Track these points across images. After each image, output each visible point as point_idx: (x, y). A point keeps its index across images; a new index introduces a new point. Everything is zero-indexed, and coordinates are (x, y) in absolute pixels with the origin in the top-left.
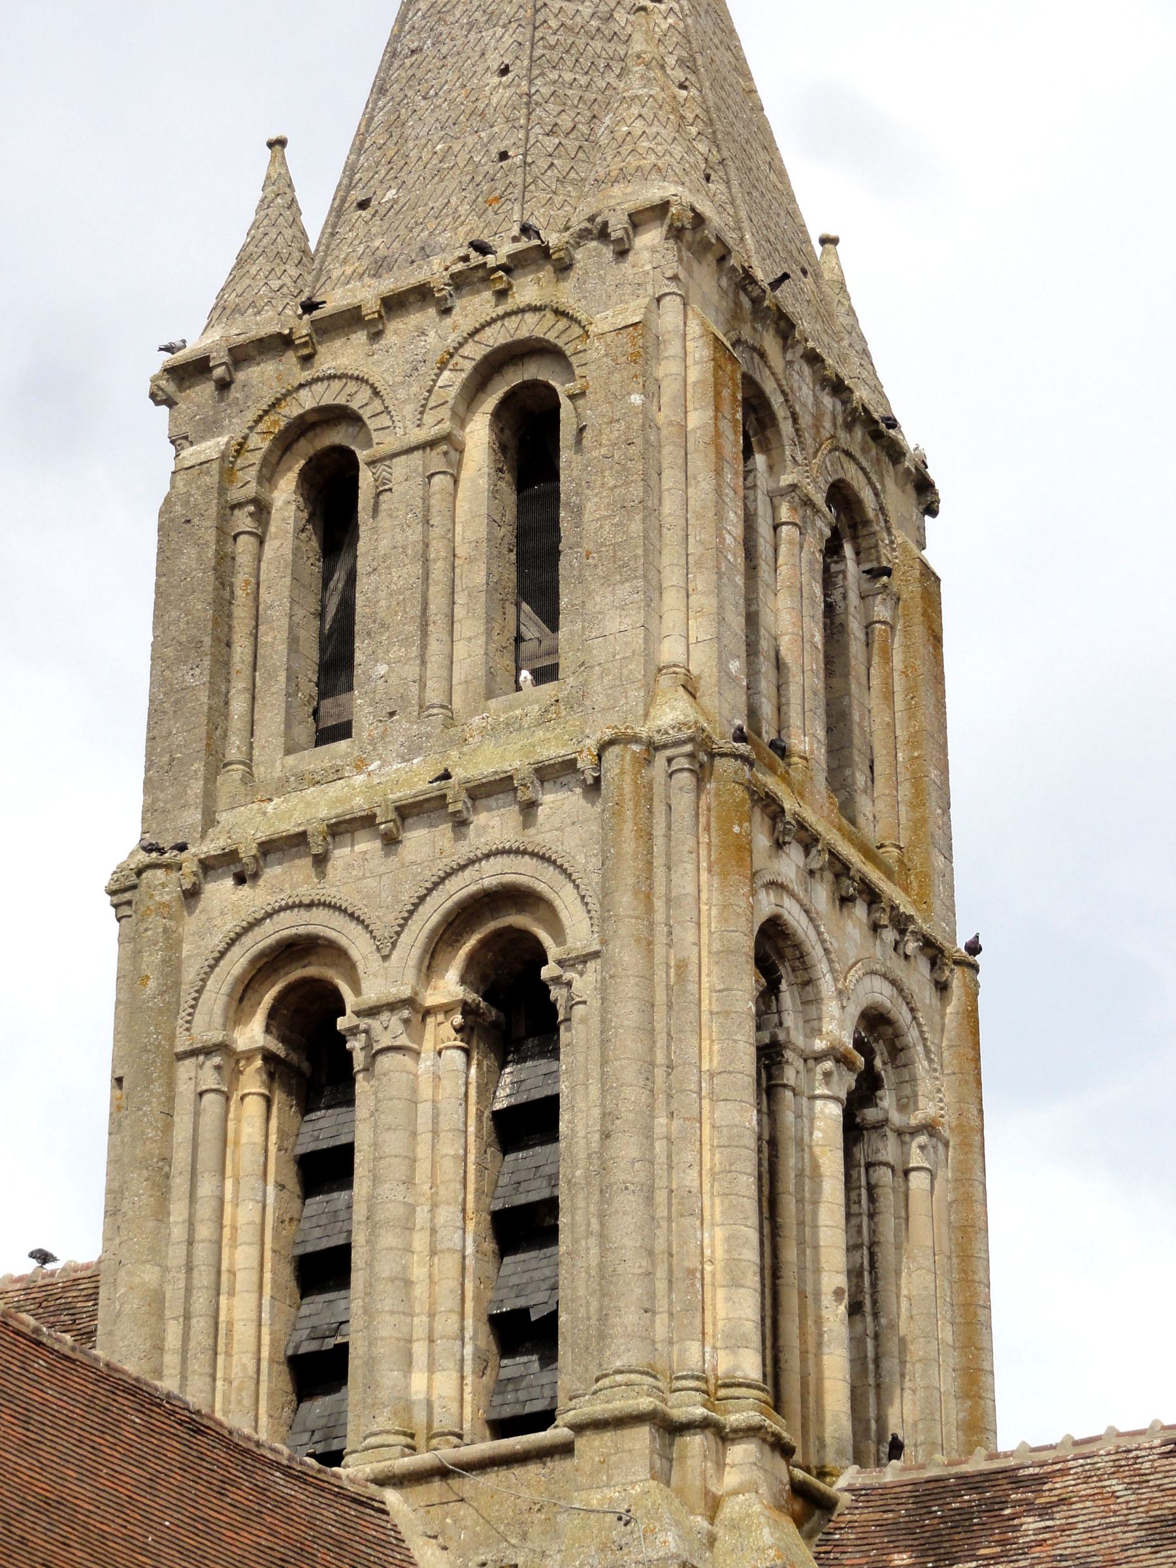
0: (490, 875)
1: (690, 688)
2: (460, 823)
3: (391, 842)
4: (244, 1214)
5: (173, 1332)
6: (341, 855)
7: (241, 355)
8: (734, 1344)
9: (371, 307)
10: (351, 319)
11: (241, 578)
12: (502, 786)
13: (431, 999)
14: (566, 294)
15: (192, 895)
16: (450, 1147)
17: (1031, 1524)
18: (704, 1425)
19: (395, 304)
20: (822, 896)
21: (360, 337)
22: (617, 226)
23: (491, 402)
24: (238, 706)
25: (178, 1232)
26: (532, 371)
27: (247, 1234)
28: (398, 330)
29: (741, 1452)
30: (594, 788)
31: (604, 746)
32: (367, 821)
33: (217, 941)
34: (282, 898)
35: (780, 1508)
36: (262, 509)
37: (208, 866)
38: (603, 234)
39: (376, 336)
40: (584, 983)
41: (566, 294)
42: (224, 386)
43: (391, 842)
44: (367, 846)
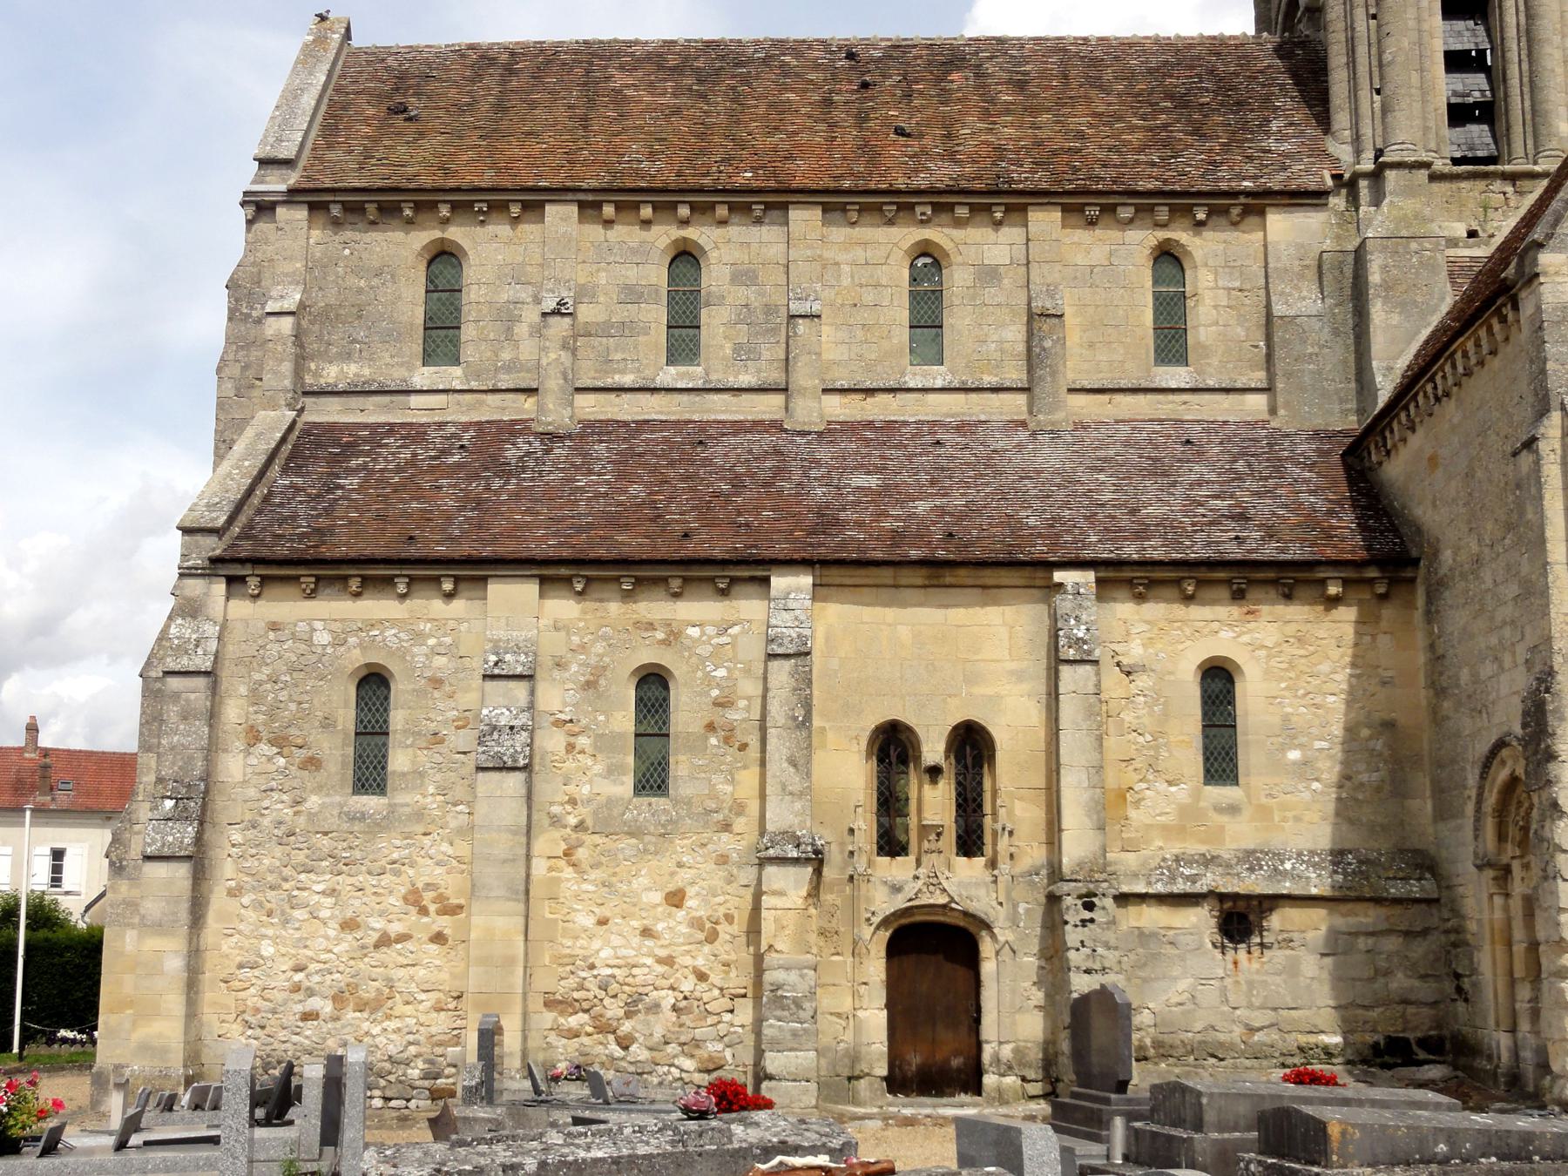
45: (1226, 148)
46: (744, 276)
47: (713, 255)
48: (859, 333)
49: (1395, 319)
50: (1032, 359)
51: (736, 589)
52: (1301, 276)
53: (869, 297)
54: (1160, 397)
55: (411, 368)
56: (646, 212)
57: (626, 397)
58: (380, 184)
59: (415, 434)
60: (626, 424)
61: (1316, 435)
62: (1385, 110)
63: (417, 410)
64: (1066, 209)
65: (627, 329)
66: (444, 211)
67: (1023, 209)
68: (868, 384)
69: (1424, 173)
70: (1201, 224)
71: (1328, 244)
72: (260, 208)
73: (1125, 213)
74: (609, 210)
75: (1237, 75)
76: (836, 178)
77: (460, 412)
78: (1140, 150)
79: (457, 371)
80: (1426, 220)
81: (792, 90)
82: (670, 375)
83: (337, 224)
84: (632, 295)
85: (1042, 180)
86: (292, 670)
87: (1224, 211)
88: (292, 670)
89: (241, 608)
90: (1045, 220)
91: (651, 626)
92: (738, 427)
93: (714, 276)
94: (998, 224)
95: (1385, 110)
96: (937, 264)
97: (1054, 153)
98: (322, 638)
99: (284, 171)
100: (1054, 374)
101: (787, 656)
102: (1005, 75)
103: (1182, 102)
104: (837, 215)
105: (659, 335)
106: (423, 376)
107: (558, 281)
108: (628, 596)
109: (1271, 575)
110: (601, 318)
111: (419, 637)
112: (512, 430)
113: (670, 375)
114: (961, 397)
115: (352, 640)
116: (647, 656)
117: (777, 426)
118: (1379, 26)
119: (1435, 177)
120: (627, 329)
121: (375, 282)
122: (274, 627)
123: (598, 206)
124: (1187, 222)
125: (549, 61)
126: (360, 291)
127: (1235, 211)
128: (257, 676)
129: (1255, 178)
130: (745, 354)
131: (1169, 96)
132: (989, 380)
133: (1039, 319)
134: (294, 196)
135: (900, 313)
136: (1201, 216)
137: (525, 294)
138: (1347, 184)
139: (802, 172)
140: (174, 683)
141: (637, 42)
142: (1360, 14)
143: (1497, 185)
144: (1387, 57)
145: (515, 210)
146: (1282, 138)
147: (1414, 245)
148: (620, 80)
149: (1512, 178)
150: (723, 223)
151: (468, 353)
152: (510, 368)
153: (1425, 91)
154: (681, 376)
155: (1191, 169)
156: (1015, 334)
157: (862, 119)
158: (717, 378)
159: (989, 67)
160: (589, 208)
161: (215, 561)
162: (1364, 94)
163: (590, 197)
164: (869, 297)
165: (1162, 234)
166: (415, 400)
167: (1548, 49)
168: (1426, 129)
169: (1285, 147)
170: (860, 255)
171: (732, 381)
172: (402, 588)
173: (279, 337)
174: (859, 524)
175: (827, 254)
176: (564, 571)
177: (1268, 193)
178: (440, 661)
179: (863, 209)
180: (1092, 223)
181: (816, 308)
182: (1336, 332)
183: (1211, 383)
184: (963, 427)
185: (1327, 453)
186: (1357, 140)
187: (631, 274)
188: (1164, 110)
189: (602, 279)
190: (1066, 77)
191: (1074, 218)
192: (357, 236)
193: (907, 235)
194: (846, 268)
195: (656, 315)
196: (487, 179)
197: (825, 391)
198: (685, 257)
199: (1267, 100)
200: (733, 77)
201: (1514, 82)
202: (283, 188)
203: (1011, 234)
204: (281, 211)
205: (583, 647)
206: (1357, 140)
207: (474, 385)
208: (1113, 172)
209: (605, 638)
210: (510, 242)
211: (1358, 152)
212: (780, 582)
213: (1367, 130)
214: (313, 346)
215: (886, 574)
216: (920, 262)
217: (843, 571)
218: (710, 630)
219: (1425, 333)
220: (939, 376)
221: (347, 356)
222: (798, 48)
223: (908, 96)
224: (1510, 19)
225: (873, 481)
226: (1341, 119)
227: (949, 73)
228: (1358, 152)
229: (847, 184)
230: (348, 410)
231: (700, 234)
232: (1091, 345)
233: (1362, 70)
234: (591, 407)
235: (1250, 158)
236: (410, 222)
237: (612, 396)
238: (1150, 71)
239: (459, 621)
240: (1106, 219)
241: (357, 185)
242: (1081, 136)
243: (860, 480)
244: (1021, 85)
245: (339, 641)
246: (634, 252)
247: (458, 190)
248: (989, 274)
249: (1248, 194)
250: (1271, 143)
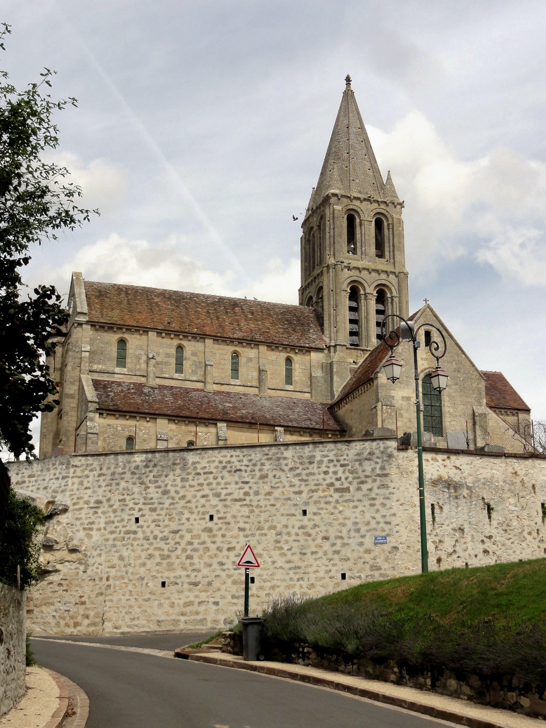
0: (383, 282)
2: (379, 274)
3: (370, 273)
6: (363, 272)
7: (343, 196)
9: (362, 199)
10: (358, 199)
12: (386, 272)
14: (388, 209)
15: (342, 270)
21: (359, 202)
22: (396, 204)
23: (375, 218)
26: (380, 216)
28: (365, 203)
30: (397, 276)
31: (400, 273)
32: (368, 270)
34: (355, 275)
37: (345, 267)
38: (393, 203)
39: (361, 202)
40: (396, 300)
41: (388, 209)
42: (339, 199)
43: (370, 273)
44: (366, 272)
45: (301, 336)
46: (194, 354)
47: (187, 348)
48: (220, 370)
49: (339, 380)
50: (260, 380)
51: (210, 425)
52: (318, 368)
53: (223, 362)
54: (286, 392)
56: (172, 336)
57: (166, 380)
58: (109, 322)
59: (119, 384)
60: (168, 386)
61: (321, 404)
62: (337, 332)
63: (117, 378)
64: (268, 346)
65: (167, 364)
66: (124, 330)
67: (258, 345)
68: (222, 383)
69: (345, 347)
70: (297, 353)
71: (324, 361)
73: (280, 349)
74: (164, 335)
75: (301, 317)
76: (216, 333)
77: (127, 380)
78: (283, 334)
79: (125, 369)
80: (345, 358)
81: (199, 308)
82: (176, 376)
83: (97, 330)
84: (168, 355)
85: (262, 339)
86: (113, 435)
87: (302, 351)
88: (113, 435)
89: (102, 420)
90: (263, 349)
91: (191, 432)
92: (195, 390)
93: (187, 353)
94: (252, 348)
95: (337, 332)
96: (237, 355)
97: (264, 332)
98: (119, 428)
99: (85, 316)
100: (265, 384)
101: (223, 440)
102: (248, 310)
103: (290, 323)
104: (216, 342)
105: (173, 366)
106: (117, 370)
107: (152, 350)
108: (186, 425)
109: (318, 432)
110: (161, 360)
112: (141, 385)
113: (176, 376)
114: (243, 387)
115: (126, 430)
117: (202, 390)
118: (336, 313)
119: (347, 348)
120: (167, 364)
121: (106, 345)
122: (109, 425)
123: (161, 333)
124: (293, 352)
125: (136, 292)
126: (102, 347)
127: (304, 351)
128: (105, 436)
129: (308, 344)
130: (194, 372)
131: (287, 321)
132: (249, 384)
133: (261, 372)
134: (87, 322)
135: (229, 366)
136: (297, 351)
137: (143, 353)
138: (329, 348)
139: (208, 330)
140: (90, 435)
141: (157, 289)
142: (332, 309)
143: (359, 352)
144: (338, 320)
145: (141, 332)
146: (313, 334)
147: (343, 364)
148: (156, 300)
149: (363, 350)
150: (190, 340)
151: (128, 365)
152: (139, 370)
153: (345, 329)
154: (180, 376)
155: (294, 339)
156: (255, 374)
157: (218, 318)
158: (188, 377)
159: (244, 307)
160: (159, 333)
161: (97, 409)
162: (332, 327)
163: (160, 331)
164: (223, 362)
165: (288, 355)
166: (116, 376)
167: (371, 322)
168: (345, 337)
169: (314, 337)
170: (221, 351)
171: (191, 379)
172: (138, 419)
173: (85, 357)
174: (233, 414)
175: (214, 351)
176: (174, 418)
177: (312, 348)
178: (146, 436)
179: (223, 341)
180: (273, 350)
181: (212, 363)
182: (325, 381)
183: (298, 390)
184: (244, 395)
185: (324, 408)
186: (330, 337)
187: (168, 350)
188: (286, 324)
189: (161, 351)
190: (262, 312)
191: (269, 348)
192: (102, 334)
193: (231, 348)
194: (217, 355)
195: (173, 361)
196: (134, 324)
197: (214, 383)
198: (180, 348)
199: (308, 324)
200: (184, 302)
201: (363, 328)
202: (85, 320)
203: (255, 351)
204: (84, 326)
205: (176, 435)
206: (330, 337)
207: (130, 373)
208: (277, 339)
209: (181, 434)
210: (139, 340)
211: (331, 340)
212: (219, 425)
213: (332, 336)
215: (240, 425)
216: (234, 355)
217: (232, 423)
218: (204, 434)
219: (345, 383)
220: (238, 382)
221: (99, 363)
222: (197, 296)
223: (227, 313)
224: (363, 314)
225: (231, 405)
226: (326, 332)
227: (235, 308)
228: (331, 340)
229: (219, 335)
230: (99, 376)
231: (184, 343)
232: (272, 379)
233: (332, 321)
234: (159, 382)
235: (307, 339)
236: (115, 332)
237: (163, 379)
238: (282, 313)
239: (150, 427)
240: (276, 350)
241: (103, 321)
242: (268, 328)
243: (227, 404)
244: (252, 313)
245: (123, 430)
246: (169, 345)
247: (127, 326)
248: (250, 360)
249: (307, 347)
250: (310, 335)
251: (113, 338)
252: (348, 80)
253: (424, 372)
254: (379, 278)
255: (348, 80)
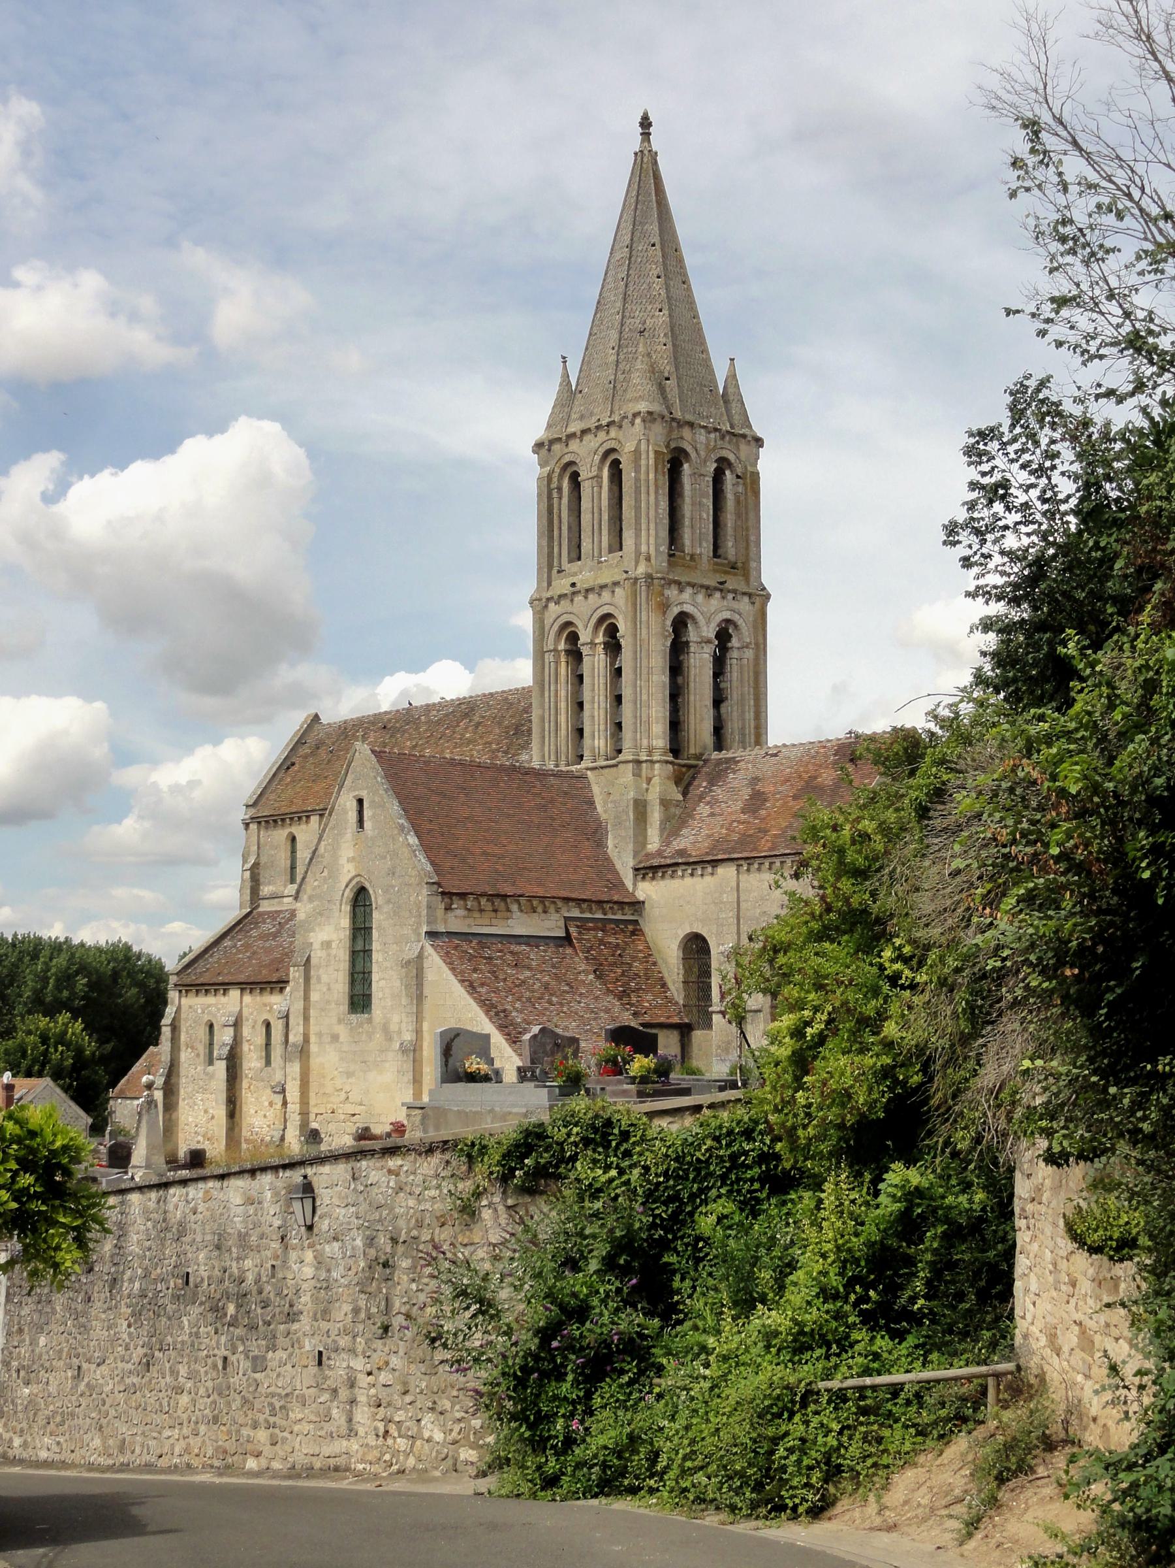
1: (648, 559)
3: (586, 597)
4: (563, 693)
5: (547, 725)
7: (552, 442)
8: (658, 738)
11: (555, 511)
13: (597, 641)
14: (621, 436)
15: (546, 606)
16: (602, 681)
17: (731, 776)
18: (646, 761)
19: (584, 432)
20: (700, 598)
24: (556, 550)
25: (547, 700)
27: (563, 699)
28: (588, 438)
29: (657, 766)
33: (551, 620)
35: (668, 778)
36: (560, 489)
37: (548, 600)
42: (549, 450)
55: (285, 886)
72: (247, 825)
89: (183, 1000)
91: (265, 1005)
111: (219, 1010)
116: (266, 1016)
122: (190, 1007)
166: (286, 900)
214: (262, 880)
221: (269, 884)
251: (280, 835)
252: (646, 123)
253: (350, 886)
254: (600, 602)
255: (646, 123)
